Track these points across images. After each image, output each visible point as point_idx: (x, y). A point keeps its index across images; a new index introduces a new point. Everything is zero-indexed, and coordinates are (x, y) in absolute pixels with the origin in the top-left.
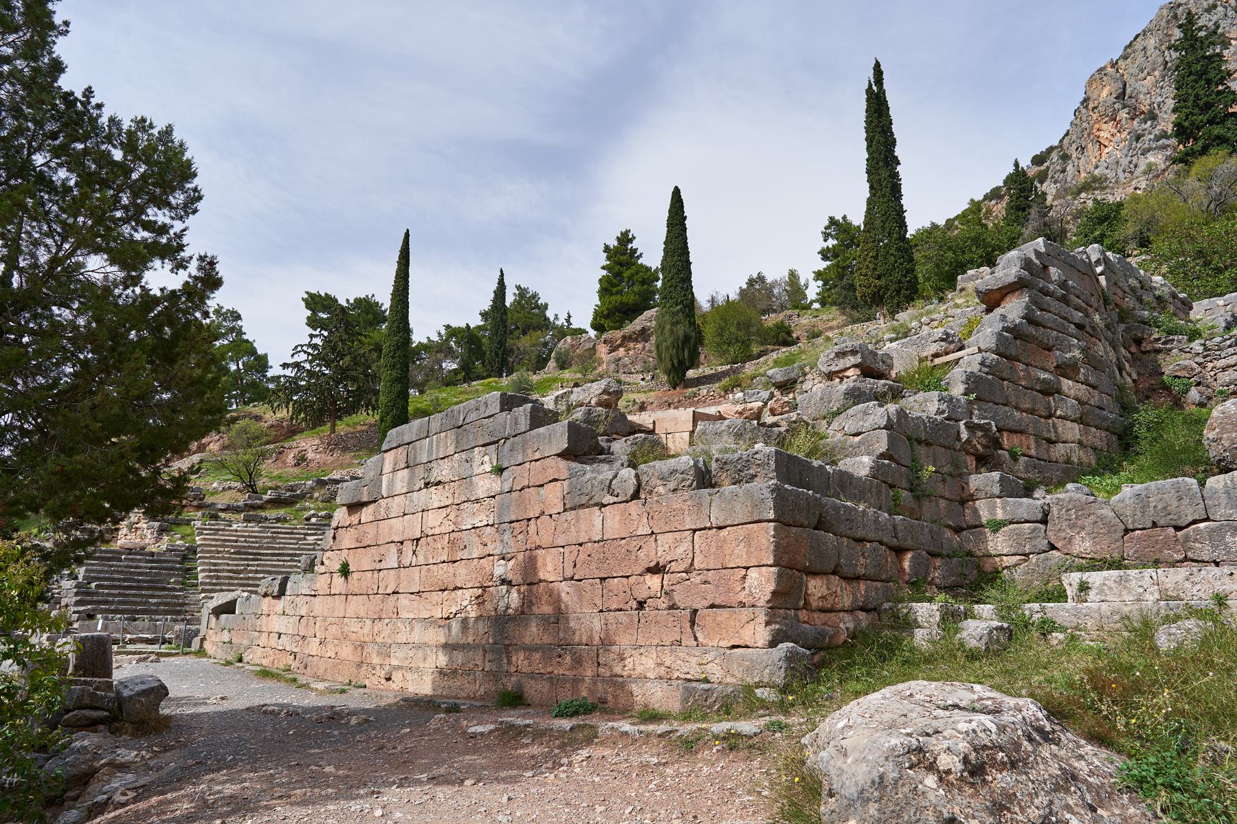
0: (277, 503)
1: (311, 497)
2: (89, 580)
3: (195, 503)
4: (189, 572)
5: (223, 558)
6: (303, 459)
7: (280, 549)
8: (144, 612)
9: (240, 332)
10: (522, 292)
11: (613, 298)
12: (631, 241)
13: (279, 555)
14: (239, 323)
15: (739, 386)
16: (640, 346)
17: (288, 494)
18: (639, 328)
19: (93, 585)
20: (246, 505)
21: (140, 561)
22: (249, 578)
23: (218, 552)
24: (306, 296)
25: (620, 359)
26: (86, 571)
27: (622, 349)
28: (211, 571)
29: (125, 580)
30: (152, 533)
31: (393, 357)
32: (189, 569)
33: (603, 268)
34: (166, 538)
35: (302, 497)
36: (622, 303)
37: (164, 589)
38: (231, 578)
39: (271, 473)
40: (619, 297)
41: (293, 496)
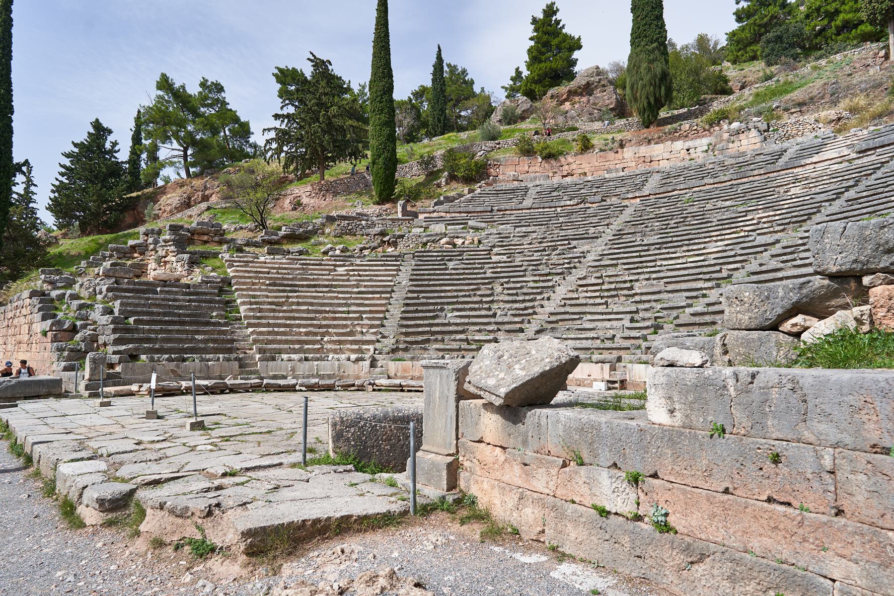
0: (292, 238)
1: (323, 233)
2: (126, 314)
3: (216, 239)
4: (229, 304)
5: (260, 290)
6: (299, 204)
7: (314, 280)
8: (192, 350)
9: (224, 103)
10: (453, 69)
11: (543, 64)
12: (555, 13)
13: (315, 286)
14: (223, 94)
15: (727, 118)
16: (584, 99)
17: (301, 230)
18: (584, 83)
19: (131, 320)
20: (263, 241)
21: (176, 293)
22: (292, 311)
23: (254, 284)
24: (276, 71)
25: (567, 112)
26: (122, 304)
27: (567, 104)
28: (251, 303)
29: (165, 314)
30: (182, 266)
31: (381, 102)
32: (228, 302)
33: (531, 39)
34: (197, 270)
35: (314, 232)
36: (551, 69)
37: (208, 324)
38: (274, 311)
39: (281, 215)
40: (548, 64)
41: (307, 232)
